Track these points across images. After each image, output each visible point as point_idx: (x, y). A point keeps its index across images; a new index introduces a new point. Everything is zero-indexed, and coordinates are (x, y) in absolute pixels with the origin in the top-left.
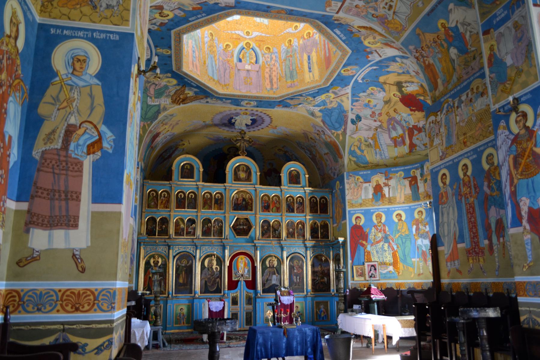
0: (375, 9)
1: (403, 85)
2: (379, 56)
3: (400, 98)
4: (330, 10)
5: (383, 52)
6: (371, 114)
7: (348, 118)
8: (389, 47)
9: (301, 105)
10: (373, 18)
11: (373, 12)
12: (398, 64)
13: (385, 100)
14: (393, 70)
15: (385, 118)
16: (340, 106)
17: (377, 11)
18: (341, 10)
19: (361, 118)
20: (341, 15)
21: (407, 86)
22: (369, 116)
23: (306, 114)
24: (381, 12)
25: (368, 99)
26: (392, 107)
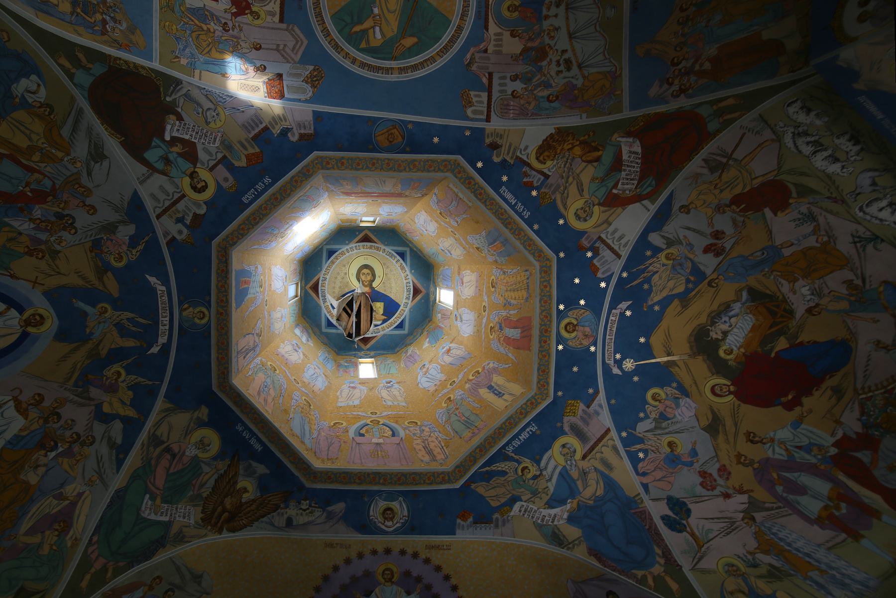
0: (547, 85)
1: (713, 335)
2: (614, 256)
3: (735, 394)
4: (474, 112)
5: (617, 235)
6: (701, 480)
7: (652, 519)
8: (620, 209)
9: (517, 506)
10: (552, 105)
11: (546, 93)
12: (662, 256)
13: (705, 423)
14: (665, 294)
15: (742, 475)
16: (611, 485)
17: (551, 86)
18: (492, 113)
19: (685, 504)
20: (496, 124)
21: (725, 334)
22: (700, 490)
23: (541, 544)
24: (559, 83)
25: (668, 438)
26: (736, 435)
